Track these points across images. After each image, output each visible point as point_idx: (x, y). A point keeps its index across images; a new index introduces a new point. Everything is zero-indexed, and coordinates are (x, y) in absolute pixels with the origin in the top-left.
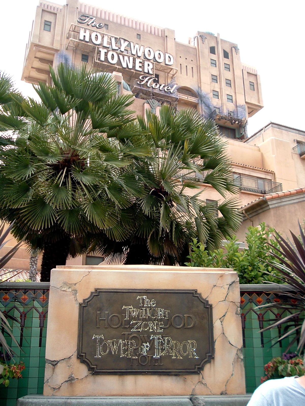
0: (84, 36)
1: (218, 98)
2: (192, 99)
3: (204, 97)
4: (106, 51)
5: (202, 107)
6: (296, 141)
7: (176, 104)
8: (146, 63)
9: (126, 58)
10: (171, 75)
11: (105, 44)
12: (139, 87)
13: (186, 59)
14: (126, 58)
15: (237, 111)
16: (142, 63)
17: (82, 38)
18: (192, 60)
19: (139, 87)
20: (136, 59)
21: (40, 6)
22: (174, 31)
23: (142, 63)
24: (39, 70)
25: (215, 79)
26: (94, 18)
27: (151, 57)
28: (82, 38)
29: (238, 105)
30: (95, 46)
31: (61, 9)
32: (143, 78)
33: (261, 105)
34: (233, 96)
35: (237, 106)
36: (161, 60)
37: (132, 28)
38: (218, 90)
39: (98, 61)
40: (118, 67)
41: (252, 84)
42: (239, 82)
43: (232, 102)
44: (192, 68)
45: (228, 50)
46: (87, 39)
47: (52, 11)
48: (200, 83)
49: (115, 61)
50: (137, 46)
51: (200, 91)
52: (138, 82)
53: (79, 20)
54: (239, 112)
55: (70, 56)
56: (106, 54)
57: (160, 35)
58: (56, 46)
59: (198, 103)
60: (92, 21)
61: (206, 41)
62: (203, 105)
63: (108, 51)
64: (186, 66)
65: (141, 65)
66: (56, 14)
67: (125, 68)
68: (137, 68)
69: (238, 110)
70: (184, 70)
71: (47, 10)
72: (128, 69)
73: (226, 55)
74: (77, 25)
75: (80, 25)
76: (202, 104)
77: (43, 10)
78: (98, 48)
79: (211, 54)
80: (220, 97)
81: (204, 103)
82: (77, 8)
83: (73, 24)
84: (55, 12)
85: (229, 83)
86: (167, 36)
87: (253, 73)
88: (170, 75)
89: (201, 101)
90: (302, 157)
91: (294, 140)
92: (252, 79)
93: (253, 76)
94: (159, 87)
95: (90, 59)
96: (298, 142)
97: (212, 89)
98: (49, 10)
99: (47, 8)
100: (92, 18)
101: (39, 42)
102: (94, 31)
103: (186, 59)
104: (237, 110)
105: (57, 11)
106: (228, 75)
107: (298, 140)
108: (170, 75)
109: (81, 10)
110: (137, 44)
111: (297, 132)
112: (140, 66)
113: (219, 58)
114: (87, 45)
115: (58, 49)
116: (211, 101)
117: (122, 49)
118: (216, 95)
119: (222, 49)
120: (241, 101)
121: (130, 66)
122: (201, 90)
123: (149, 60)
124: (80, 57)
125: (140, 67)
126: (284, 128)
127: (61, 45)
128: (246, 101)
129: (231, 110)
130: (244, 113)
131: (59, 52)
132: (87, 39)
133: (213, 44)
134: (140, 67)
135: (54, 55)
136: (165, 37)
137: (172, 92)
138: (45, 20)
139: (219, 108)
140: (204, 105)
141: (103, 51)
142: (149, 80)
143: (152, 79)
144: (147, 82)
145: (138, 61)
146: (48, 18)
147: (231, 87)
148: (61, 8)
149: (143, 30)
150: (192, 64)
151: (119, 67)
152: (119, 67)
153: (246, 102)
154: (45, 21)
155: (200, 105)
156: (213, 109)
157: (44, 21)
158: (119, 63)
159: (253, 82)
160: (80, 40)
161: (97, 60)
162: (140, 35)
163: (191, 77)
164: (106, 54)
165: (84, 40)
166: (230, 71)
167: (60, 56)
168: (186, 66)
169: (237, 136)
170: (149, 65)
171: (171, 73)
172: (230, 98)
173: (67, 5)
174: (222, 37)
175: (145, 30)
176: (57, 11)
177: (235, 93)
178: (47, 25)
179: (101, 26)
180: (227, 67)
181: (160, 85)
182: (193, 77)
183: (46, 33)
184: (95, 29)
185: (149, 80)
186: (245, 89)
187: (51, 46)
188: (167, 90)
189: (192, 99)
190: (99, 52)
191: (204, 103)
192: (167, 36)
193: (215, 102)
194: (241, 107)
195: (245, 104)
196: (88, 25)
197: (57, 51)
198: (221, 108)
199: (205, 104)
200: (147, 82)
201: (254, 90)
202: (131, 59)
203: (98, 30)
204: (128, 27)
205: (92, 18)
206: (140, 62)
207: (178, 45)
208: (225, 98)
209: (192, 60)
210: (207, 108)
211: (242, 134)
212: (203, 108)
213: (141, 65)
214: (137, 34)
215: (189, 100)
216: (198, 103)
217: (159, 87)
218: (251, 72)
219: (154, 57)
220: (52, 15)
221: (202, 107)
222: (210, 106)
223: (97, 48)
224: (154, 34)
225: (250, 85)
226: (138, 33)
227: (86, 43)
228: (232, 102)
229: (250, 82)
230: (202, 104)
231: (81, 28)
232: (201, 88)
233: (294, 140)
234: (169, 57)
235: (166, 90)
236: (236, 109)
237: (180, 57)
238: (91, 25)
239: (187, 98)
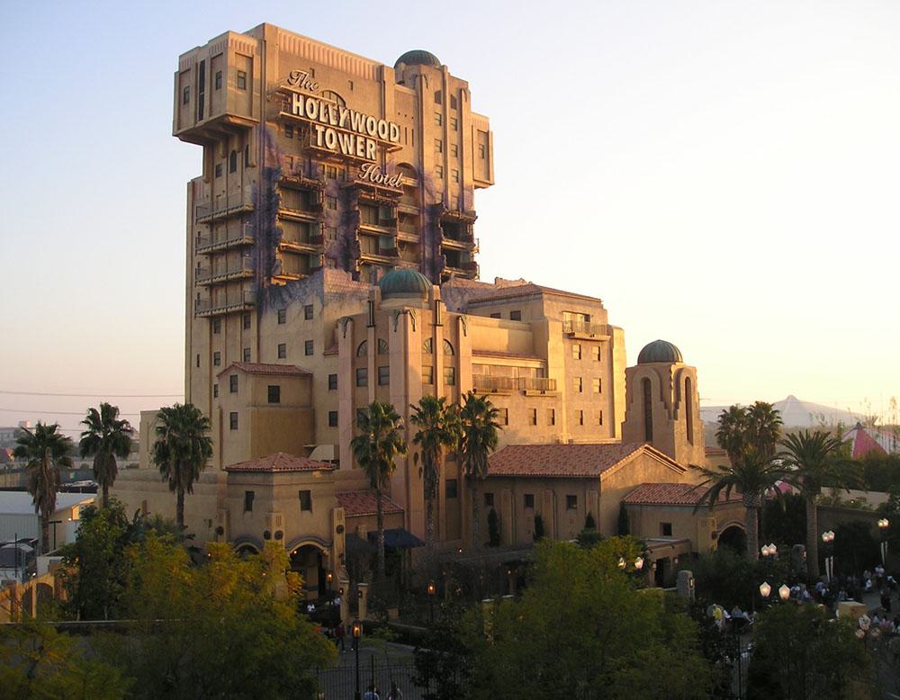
8: (369, 142)
9: (346, 136)
23: (365, 144)
56: (324, 133)
63: (326, 128)
68: (360, 154)
101: (236, 111)
102: (309, 97)
122: (423, 168)
125: (362, 150)
132: (301, 113)
141: (320, 129)
145: (360, 139)
163: (411, 147)
164: (324, 133)
165: (298, 115)
170: (372, 146)
199: (427, 190)
206: (362, 143)
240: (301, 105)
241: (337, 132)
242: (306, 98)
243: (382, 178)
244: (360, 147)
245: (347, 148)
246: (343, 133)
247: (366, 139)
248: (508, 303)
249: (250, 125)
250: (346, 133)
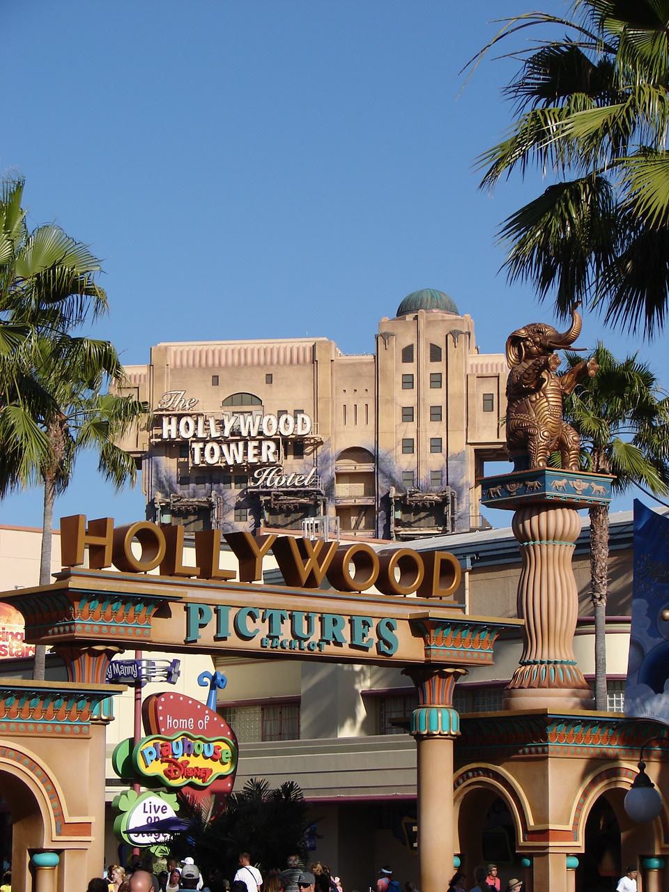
2: (367, 467)
8: (265, 444)
9: (233, 446)
11: (201, 434)
14: (233, 446)
20: (249, 443)
23: (259, 447)
25: (408, 414)
32: (259, 474)
42: (457, 408)
45: (440, 343)
56: (203, 450)
65: (256, 452)
70: (351, 416)
81: (382, 472)
94: (286, 482)
103: (355, 390)
106: (436, 397)
117: (227, 433)
118: (408, 446)
132: (174, 436)
134: (255, 455)
141: (197, 447)
142: (268, 474)
144: (266, 479)
145: (251, 444)
164: (203, 450)
170: (269, 447)
180: (436, 381)
185: (268, 474)
189: (367, 467)
191: (382, 472)
193: (402, 463)
194: (461, 457)
195: (464, 447)
200: (266, 479)
202: (241, 444)
206: (255, 447)
213: (256, 452)
217: (286, 482)
218: (485, 373)
222: (394, 475)
235: (296, 484)
240: (173, 427)
243: (284, 480)
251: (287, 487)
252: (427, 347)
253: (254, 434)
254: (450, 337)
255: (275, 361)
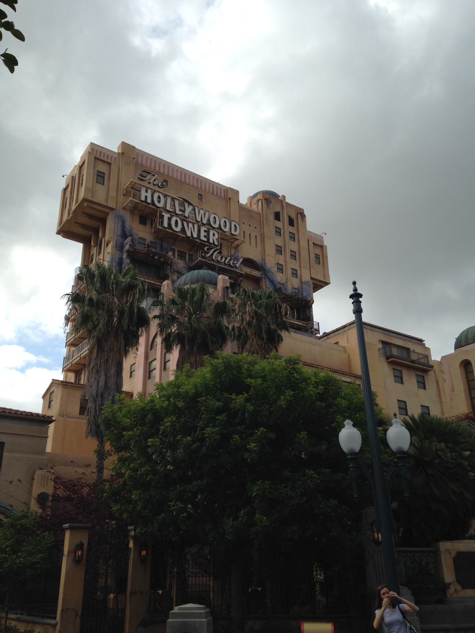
0: (146, 197)
1: (283, 273)
2: (256, 273)
3: (269, 271)
4: (169, 215)
5: (266, 283)
6: (381, 341)
7: (241, 281)
8: (211, 232)
9: (191, 225)
10: (235, 245)
12: (204, 260)
13: (250, 225)
14: (191, 225)
15: (302, 288)
16: (207, 232)
17: (143, 199)
18: (256, 228)
19: (204, 260)
20: (201, 227)
21: (91, 152)
22: (238, 192)
23: (207, 232)
24: (83, 226)
25: (279, 250)
26: (156, 176)
27: (217, 226)
28: (143, 199)
29: (303, 281)
30: (157, 208)
31: (115, 158)
32: (208, 249)
33: (327, 282)
34: (298, 271)
35: (302, 283)
36: (227, 229)
37: (193, 186)
38: (283, 263)
39: (160, 227)
40: (181, 235)
41: (317, 257)
42: (304, 254)
43: (297, 278)
44: (256, 236)
45: (293, 216)
46: (149, 201)
47: (106, 159)
48: (264, 254)
49: (178, 229)
50: (202, 212)
51: (263, 263)
52: (203, 254)
53: (139, 176)
54: (303, 289)
55: (127, 217)
56: (170, 219)
57: (223, 196)
58: (111, 204)
59: (261, 278)
60: (154, 178)
61: (271, 206)
62: (267, 280)
63: (172, 216)
64: (250, 234)
65: (206, 234)
66: (110, 164)
67: (189, 237)
68: (202, 238)
69: (303, 287)
70: (247, 238)
71: (100, 158)
72: (191, 238)
73: (291, 222)
74: (137, 182)
75: (140, 182)
76: (265, 279)
77: (95, 158)
78: (161, 212)
79: (276, 221)
80: (284, 272)
81: (268, 278)
82: (134, 158)
83: (133, 180)
84: (109, 161)
85: (293, 255)
86: (230, 198)
87: (319, 244)
88: (234, 245)
89: (265, 276)
90: (389, 360)
91: (379, 340)
92: (318, 251)
93: (319, 247)
94: (225, 261)
95: (148, 223)
96: (383, 343)
97: (276, 262)
98: (102, 158)
99: (100, 155)
100: (154, 175)
101: (92, 197)
104: (302, 286)
105: (111, 159)
106: (293, 246)
107: (383, 340)
108: (234, 245)
109: (137, 160)
110: (202, 209)
111: (382, 331)
112: (205, 235)
113: (284, 225)
114: (148, 206)
115: (114, 207)
116: (275, 276)
119: (287, 213)
120: (306, 277)
121: (195, 235)
122: (265, 263)
123: (214, 228)
124: (137, 219)
125: (205, 236)
126: (369, 327)
127: (117, 202)
128: (313, 276)
129: (296, 286)
130: (309, 291)
131: (114, 212)
132: (149, 201)
133: (278, 209)
134: (205, 236)
135: (108, 214)
136: (228, 198)
137: (237, 266)
138: (98, 170)
139: (283, 284)
140: (268, 280)
141: (166, 216)
143: (217, 252)
144: (212, 254)
145: (203, 229)
146: (102, 168)
147: (296, 260)
148: (116, 156)
149: (205, 190)
150: (256, 232)
151: (183, 235)
152: (183, 235)
153: (312, 278)
154: (98, 171)
155: (264, 281)
156: (279, 286)
157: (96, 172)
158: (183, 230)
159: (319, 254)
160: (141, 201)
161: (159, 226)
162: (201, 195)
163: (255, 248)
164: (170, 219)
165: (146, 201)
166: (295, 241)
167: (116, 216)
168: (250, 234)
169: (301, 317)
170: (214, 235)
171: (236, 243)
172: (295, 273)
173: (123, 153)
174: (287, 200)
175: (207, 190)
176: (111, 159)
177: (300, 267)
178: (100, 177)
179: (164, 185)
180: (292, 237)
181: (226, 259)
182: (256, 247)
183: (99, 186)
184: (156, 188)
186: (311, 262)
187: (105, 204)
188: (233, 264)
189: (256, 273)
190: (162, 217)
191: (268, 278)
192: (230, 198)
193: (279, 277)
194: (306, 283)
195: (310, 279)
196: (149, 183)
197: (112, 209)
198: (285, 285)
200: (212, 254)
201: (320, 264)
202: (196, 226)
203: (161, 190)
204: (189, 185)
205: (154, 175)
206: (205, 231)
207: (241, 208)
208: (290, 272)
209: (256, 228)
210: (271, 284)
211: (307, 315)
212: (267, 284)
214: (199, 194)
215: (252, 274)
216: (261, 278)
217: (225, 261)
218: (317, 243)
219: (220, 225)
220: (106, 164)
221: (266, 283)
222: (275, 282)
223: (159, 211)
224: (216, 195)
225: (316, 257)
226: (200, 193)
227: (148, 205)
228: (297, 278)
229: (315, 254)
230: (265, 279)
231: (142, 187)
232: (265, 261)
233: (379, 340)
234: (235, 226)
235: (232, 264)
236: (300, 285)
237: (244, 223)
238: (152, 184)
239: (250, 272)
241: (182, 221)
242: (154, 192)
243: (224, 259)
244: (203, 234)
245: (191, 231)
246: (188, 222)
247: (209, 229)
248: (328, 339)
249: (107, 211)
250: (191, 222)
251: (225, 264)
252: (287, 216)
253: (205, 221)
254: (299, 216)
255: (203, 188)
